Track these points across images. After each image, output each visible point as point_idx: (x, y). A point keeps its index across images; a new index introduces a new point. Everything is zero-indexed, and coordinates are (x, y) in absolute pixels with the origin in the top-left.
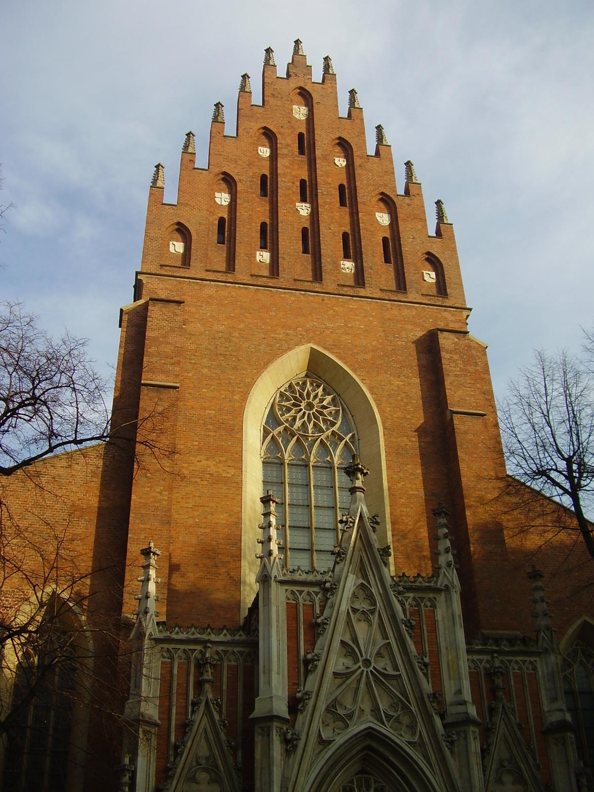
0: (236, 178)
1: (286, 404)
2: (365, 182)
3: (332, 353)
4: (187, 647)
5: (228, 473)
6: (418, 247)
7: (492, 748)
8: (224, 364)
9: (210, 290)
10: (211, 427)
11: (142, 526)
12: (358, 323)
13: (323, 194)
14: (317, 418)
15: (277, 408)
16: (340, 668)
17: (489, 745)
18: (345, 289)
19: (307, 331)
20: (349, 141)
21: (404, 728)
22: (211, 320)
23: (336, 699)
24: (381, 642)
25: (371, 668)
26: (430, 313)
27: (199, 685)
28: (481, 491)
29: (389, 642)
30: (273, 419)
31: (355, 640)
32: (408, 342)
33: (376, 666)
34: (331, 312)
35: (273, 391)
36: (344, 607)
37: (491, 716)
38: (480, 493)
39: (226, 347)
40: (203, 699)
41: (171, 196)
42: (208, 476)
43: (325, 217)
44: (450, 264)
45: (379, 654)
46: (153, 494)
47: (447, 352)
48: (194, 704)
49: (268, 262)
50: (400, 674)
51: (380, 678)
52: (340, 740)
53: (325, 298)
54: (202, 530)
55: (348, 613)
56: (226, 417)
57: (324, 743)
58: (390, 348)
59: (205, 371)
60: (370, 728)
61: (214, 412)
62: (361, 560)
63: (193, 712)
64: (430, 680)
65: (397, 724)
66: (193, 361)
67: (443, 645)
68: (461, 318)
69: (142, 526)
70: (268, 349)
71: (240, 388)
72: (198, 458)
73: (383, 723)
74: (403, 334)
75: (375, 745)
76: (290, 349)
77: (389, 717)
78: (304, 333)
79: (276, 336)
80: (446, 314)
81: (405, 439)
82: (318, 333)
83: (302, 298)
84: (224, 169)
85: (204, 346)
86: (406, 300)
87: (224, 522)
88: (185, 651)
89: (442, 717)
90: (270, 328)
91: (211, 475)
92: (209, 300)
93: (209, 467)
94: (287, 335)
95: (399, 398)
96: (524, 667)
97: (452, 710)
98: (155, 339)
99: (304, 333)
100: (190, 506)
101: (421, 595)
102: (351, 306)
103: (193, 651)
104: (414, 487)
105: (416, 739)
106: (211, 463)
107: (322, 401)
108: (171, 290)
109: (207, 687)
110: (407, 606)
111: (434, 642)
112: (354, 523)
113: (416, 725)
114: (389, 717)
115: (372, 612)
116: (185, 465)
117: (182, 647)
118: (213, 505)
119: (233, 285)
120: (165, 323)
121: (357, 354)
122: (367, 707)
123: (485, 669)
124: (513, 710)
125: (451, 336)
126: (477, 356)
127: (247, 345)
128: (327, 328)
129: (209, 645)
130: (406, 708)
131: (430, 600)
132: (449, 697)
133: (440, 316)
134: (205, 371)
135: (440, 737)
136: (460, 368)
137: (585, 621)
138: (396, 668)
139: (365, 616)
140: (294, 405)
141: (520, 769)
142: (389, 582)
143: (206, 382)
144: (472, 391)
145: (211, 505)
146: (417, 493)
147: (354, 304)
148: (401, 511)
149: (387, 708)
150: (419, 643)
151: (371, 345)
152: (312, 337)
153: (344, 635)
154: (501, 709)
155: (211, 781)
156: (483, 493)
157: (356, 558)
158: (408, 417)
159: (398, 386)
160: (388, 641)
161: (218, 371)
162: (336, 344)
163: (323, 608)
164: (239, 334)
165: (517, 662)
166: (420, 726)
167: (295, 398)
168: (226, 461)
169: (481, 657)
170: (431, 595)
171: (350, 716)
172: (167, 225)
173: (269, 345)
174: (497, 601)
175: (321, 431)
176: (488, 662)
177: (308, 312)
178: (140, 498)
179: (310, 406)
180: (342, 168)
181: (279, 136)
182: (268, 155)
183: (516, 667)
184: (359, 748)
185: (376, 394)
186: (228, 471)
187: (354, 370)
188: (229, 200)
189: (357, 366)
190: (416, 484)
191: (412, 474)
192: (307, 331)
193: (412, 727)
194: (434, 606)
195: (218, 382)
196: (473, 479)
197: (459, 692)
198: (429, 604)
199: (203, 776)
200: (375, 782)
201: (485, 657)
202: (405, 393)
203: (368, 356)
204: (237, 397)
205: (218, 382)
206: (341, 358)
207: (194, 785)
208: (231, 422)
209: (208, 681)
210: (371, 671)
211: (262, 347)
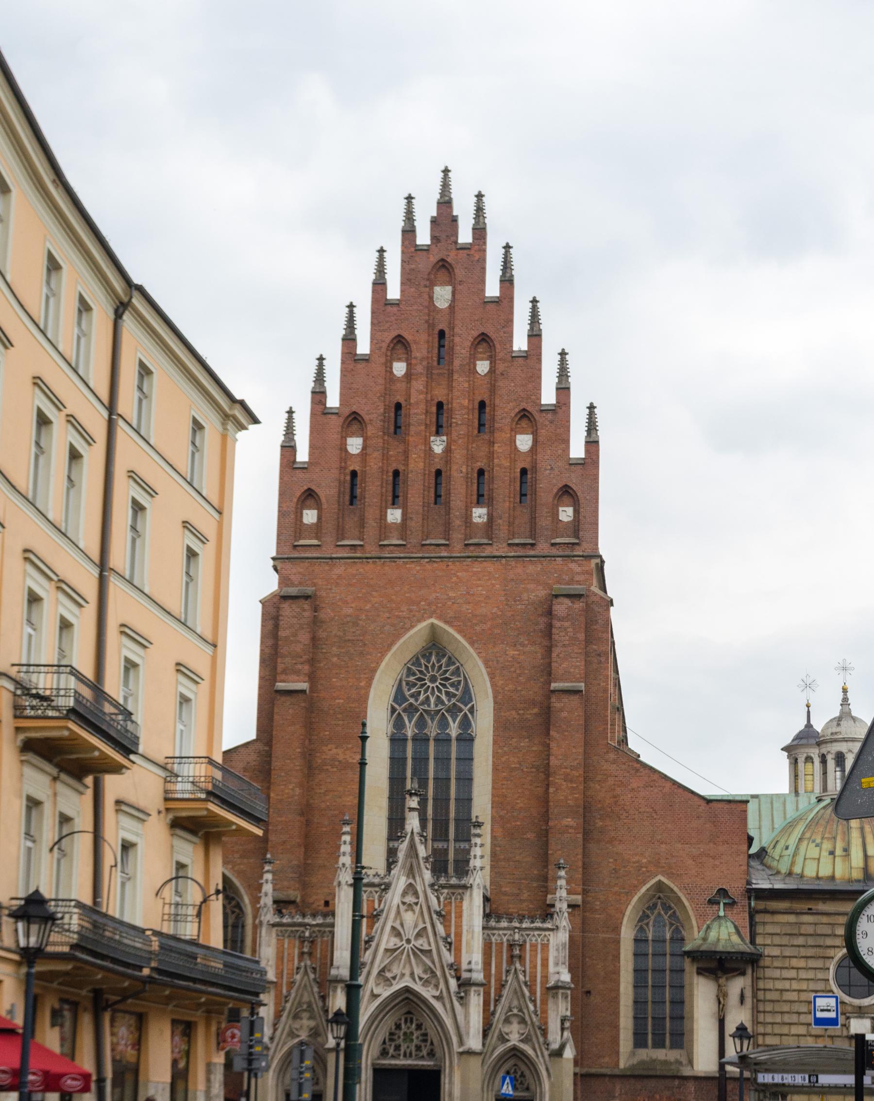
0: (366, 418)
1: (412, 679)
2: (506, 397)
3: (452, 626)
4: (294, 929)
5: (354, 759)
6: (554, 481)
7: (503, 999)
8: (352, 651)
9: (339, 570)
10: (339, 716)
11: (279, 819)
12: (480, 588)
13: (457, 424)
14: (440, 691)
15: (404, 683)
16: (391, 946)
17: (500, 996)
18: (472, 548)
19: (429, 604)
20: (492, 338)
21: (432, 986)
22: (339, 603)
23: (385, 967)
24: (421, 926)
25: (411, 945)
26: (556, 567)
27: (302, 954)
28: (567, 768)
29: (426, 927)
30: (399, 697)
31: (402, 925)
32: (528, 605)
33: (416, 944)
34: (454, 579)
35: (399, 668)
36: (397, 900)
37: (507, 976)
38: (564, 770)
39: (353, 632)
40: (302, 964)
41: (303, 455)
42: (337, 763)
43: (458, 457)
44: (588, 498)
45: (419, 935)
46: (287, 791)
47: (559, 620)
48: (298, 968)
49: (399, 521)
50: (431, 950)
51: (419, 952)
52: (386, 993)
53: (450, 564)
54: (332, 812)
55: (398, 906)
56: (354, 705)
57: (375, 996)
58: (509, 614)
59: (335, 659)
60: (406, 986)
61: (342, 701)
62: (411, 865)
63: (297, 973)
64: (453, 953)
65: (427, 984)
66: (324, 651)
67: (465, 928)
68: (588, 568)
69: (279, 819)
70: (392, 628)
71: (365, 674)
72: (330, 746)
73: (416, 983)
74: (525, 596)
75: (411, 997)
76: (412, 627)
77: (421, 979)
78: (427, 607)
79: (400, 614)
80: (573, 566)
81: (514, 712)
82: (440, 605)
83: (428, 567)
84: (354, 408)
85: (334, 632)
86: (532, 553)
87: (350, 804)
88: (292, 931)
89: (458, 978)
90: (394, 605)
91: (340, 761)
92: (338, 581)
93: (338, 755)
94: (411, 611)
95: (513, 669)
96: (539, 940)
97: (465, 975)
98: (286, 638)
99: (427, 607)
100: (322, 791)
101: (453, 891)
102: (475, 569)
103: (297, 931)
104: (516, 760)
105: (437, 994)
106: (340, 751)
107: (446, 672)
108: (304, 575)
109: (306, 956)
110: (442, 899)
111: (459, 926)
112: (405, 837)
113: (439, 984)
114: (421, 979)
115: (416, 904)
116: (318, 755)
117: (290, 929)
118: (340, 789)
119: (361, 560)
120: (295, 621)
121: (476, 624)
122: (407, 972)
123: (508, 940)
124: (524, 972)
125: (567, 601)
126: (599, 612)
127: (372, 627)
128: (450, 599)
129: (308, 927)
130: (433, 972)
131: (459, 894)
132: (464, 966)
133: (566, 568)
134: (335, 659)
135: (452, 994)
136: (570, 637)
137: (660, 880)
138: (430, 945)
139: (410, 907)
140: (419, 679)
141: (523, 1013)
142: (427, 884)
143: (334, 671)
144: (577, 662)
145: (339, 789)
146: (518, 766)
147: (477, 567)
148: (502, 784)
149: (421, 972)
150: (447, 927)
151: (492, 613)
152: (435, 611)
153: (394, 921)
154: (513, 971)
155: (310, 1018)
156: (568, 770)
157: (408, 865)
158: (519, 688)
159: (513, 657)
160: (424, 926)
161: (346, 659)
162: (457, 616)
163: (380, 901)
164: (366, 616)
165: (534, 935)
166: (442, 985)
167: (421, 672)
168: (352, 748)
169: (505, 932)
170: (460, 891)
171: (394, 978)
172: (298, 494)
173: (393, 625)
175: (443, 703)
176: (511, 935)
177: (432, 582)
178: (277, 795)
179: (433, 679)
180: (485, 375)
181: (414, 347)
182: (403, 372)
183: (534, 939)
184: (400, 999)
185: (490, 667)
186: (354, 757)
187: (472, 644)
188: (360, 447)
189: (475, 638)
190: (518, 757)
191: (516, 748)
192: (429, 604)
193: (436, 986)
194: (462, 899)
195: (347, 669)
196: (561, 757)
197: (470, 963)
198: (459, 897)
199: (305, 1015)
200: (417, 1020)
201: (509, 932)
202: (519, 663)
203: (485, 627)
204: (362, 684)
205: (347, 669)
206: (460, 632)
207: (298, 1020)
208: (358, 710)
209: (306, 953)
210: (411, 948)
211: (387, 628)
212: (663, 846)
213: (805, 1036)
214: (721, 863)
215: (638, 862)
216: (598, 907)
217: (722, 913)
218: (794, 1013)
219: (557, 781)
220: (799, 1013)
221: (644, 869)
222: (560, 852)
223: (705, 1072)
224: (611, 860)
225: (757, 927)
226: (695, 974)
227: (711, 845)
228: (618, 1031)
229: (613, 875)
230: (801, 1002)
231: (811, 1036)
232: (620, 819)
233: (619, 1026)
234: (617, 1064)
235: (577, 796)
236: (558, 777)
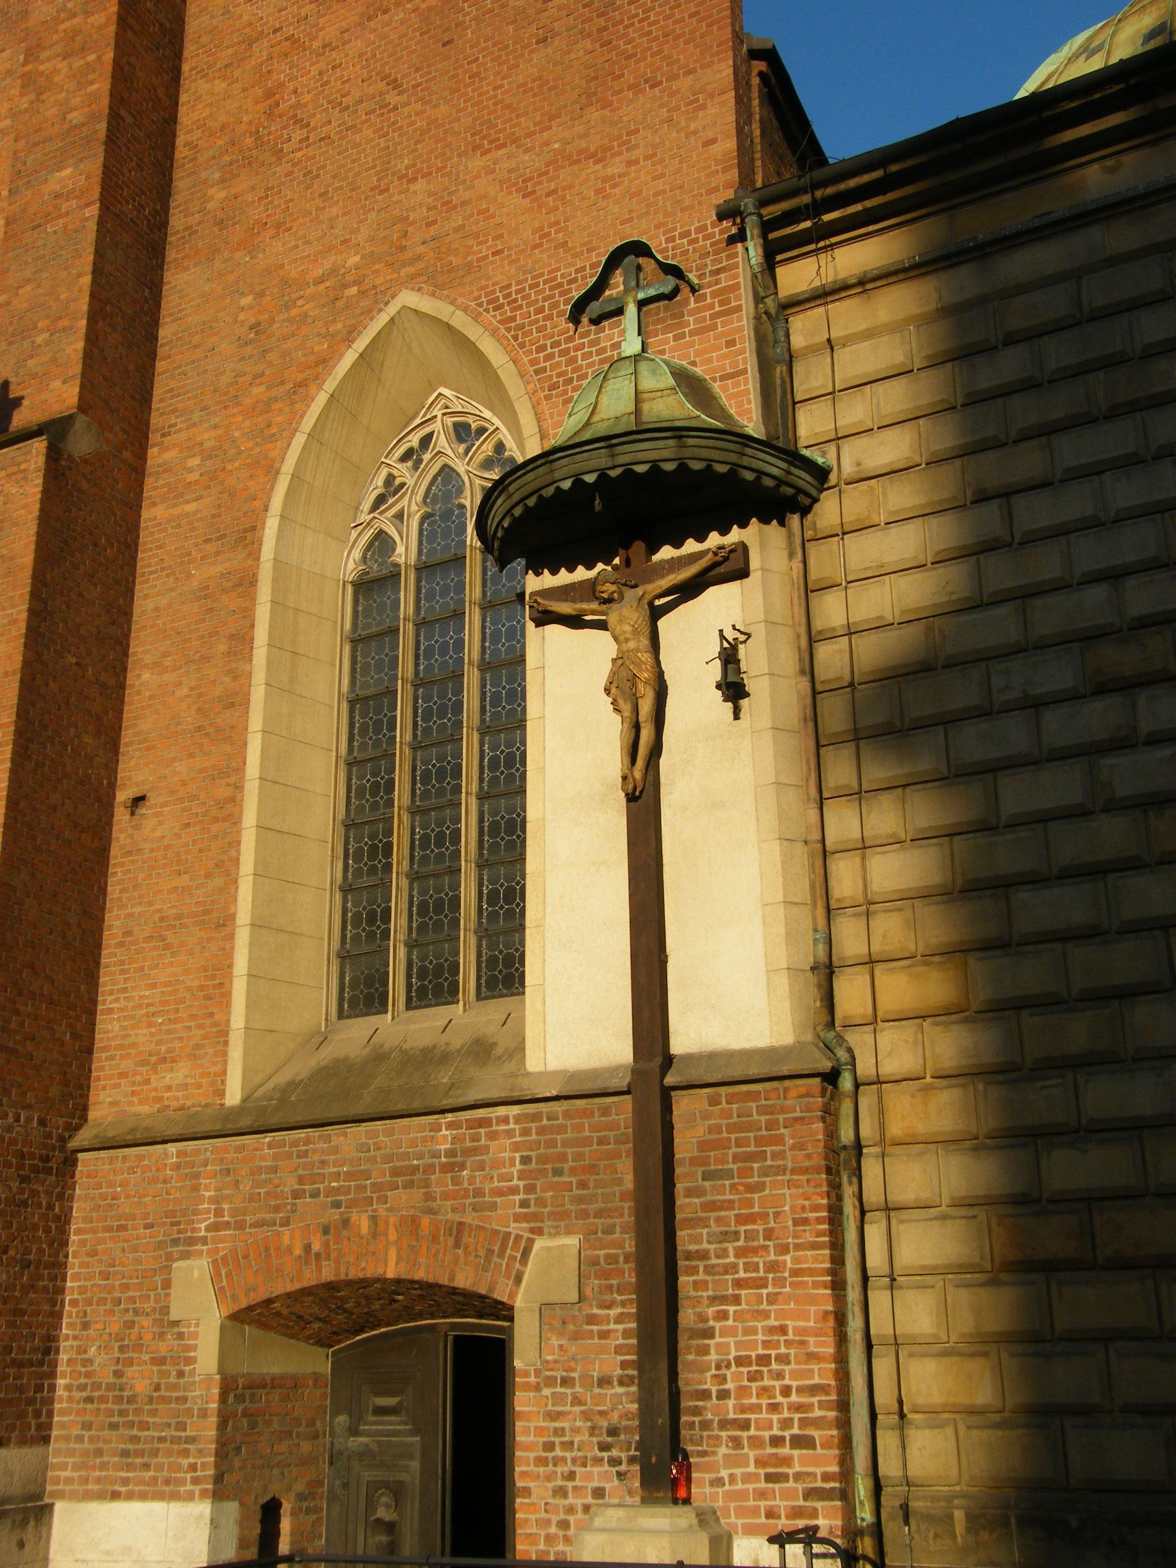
174: (40, 339)
212: (420, 186)
213: (1081, 813)
214: (630, 163)
215: (333, 272)
216: (195, 476)
217: (632, 345)
218: (1007, 709)
219: (41, 68)
220: (1034, 705)
221: (354, 290)
222: (28, 288)
223: (573, 1076)
224: (246, 301)
225: (798, 368)
226: (530, 625)
227: (594, 114)
228: (231, 937)
229: (248, 350)
230: (1041, 647)
231: (1112, 806)
232: (279, 154)
233: (233, 917)
234: (221, 1093)
235: (95, 86)
236: (46, 54)
